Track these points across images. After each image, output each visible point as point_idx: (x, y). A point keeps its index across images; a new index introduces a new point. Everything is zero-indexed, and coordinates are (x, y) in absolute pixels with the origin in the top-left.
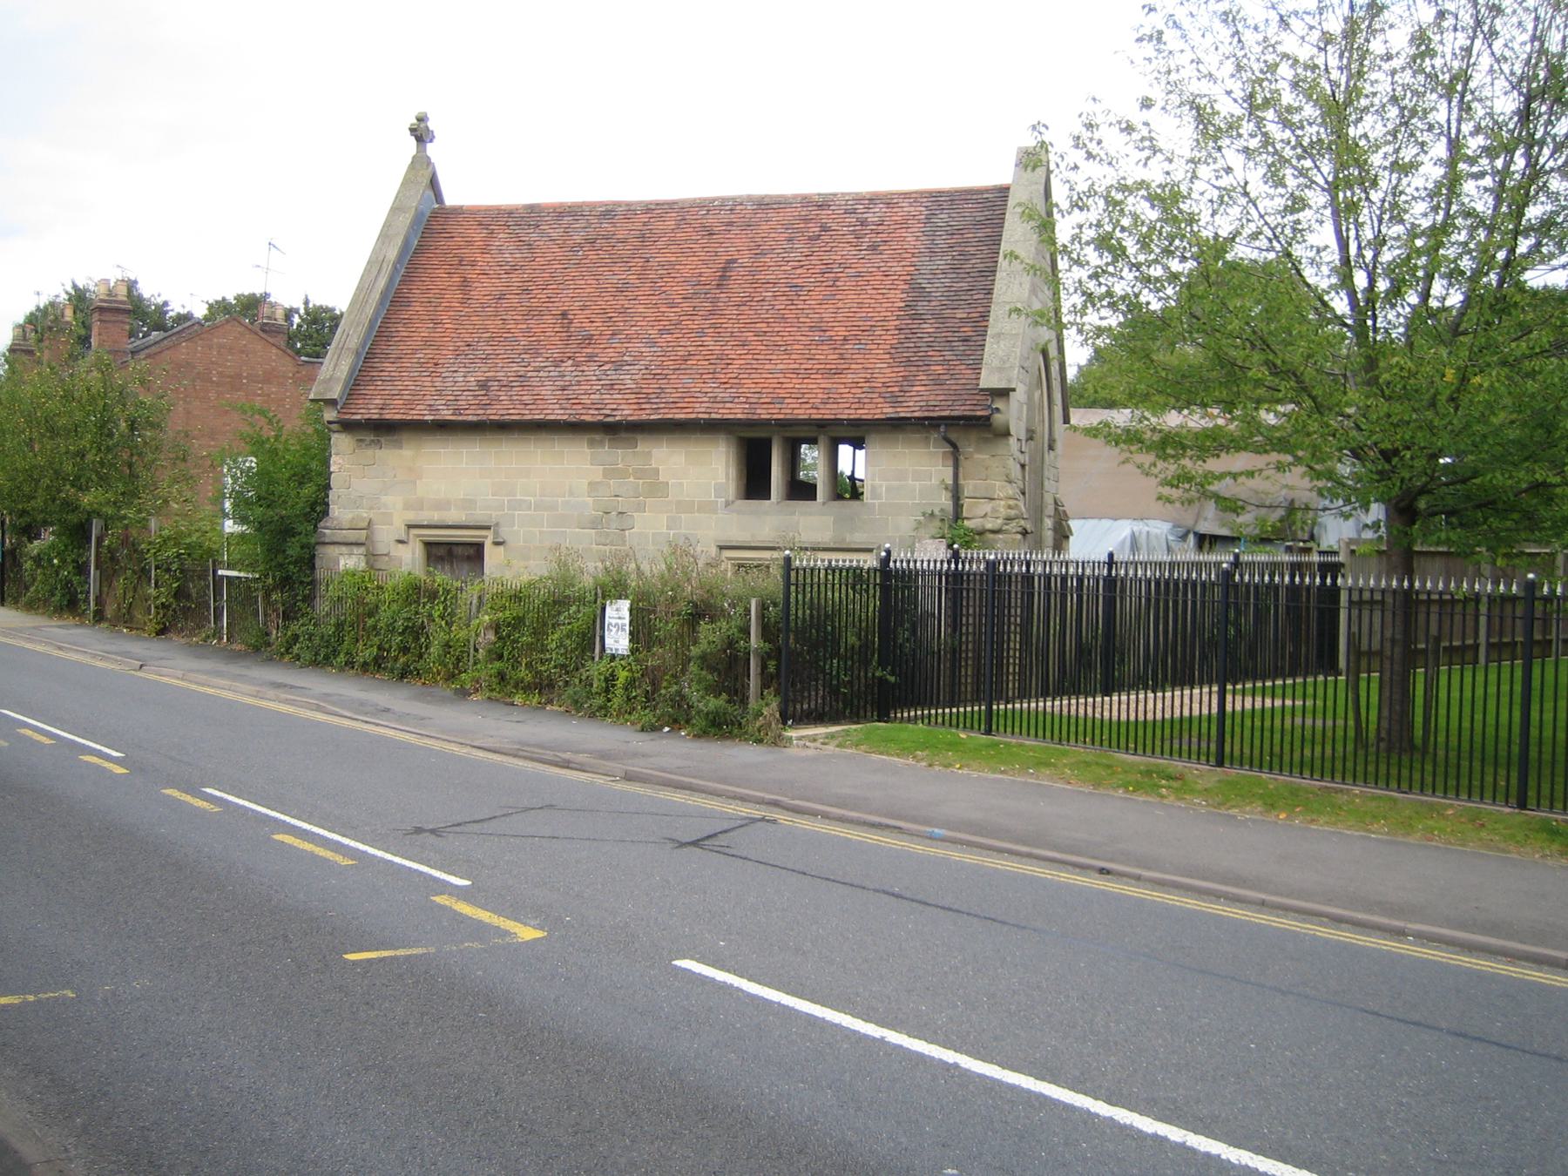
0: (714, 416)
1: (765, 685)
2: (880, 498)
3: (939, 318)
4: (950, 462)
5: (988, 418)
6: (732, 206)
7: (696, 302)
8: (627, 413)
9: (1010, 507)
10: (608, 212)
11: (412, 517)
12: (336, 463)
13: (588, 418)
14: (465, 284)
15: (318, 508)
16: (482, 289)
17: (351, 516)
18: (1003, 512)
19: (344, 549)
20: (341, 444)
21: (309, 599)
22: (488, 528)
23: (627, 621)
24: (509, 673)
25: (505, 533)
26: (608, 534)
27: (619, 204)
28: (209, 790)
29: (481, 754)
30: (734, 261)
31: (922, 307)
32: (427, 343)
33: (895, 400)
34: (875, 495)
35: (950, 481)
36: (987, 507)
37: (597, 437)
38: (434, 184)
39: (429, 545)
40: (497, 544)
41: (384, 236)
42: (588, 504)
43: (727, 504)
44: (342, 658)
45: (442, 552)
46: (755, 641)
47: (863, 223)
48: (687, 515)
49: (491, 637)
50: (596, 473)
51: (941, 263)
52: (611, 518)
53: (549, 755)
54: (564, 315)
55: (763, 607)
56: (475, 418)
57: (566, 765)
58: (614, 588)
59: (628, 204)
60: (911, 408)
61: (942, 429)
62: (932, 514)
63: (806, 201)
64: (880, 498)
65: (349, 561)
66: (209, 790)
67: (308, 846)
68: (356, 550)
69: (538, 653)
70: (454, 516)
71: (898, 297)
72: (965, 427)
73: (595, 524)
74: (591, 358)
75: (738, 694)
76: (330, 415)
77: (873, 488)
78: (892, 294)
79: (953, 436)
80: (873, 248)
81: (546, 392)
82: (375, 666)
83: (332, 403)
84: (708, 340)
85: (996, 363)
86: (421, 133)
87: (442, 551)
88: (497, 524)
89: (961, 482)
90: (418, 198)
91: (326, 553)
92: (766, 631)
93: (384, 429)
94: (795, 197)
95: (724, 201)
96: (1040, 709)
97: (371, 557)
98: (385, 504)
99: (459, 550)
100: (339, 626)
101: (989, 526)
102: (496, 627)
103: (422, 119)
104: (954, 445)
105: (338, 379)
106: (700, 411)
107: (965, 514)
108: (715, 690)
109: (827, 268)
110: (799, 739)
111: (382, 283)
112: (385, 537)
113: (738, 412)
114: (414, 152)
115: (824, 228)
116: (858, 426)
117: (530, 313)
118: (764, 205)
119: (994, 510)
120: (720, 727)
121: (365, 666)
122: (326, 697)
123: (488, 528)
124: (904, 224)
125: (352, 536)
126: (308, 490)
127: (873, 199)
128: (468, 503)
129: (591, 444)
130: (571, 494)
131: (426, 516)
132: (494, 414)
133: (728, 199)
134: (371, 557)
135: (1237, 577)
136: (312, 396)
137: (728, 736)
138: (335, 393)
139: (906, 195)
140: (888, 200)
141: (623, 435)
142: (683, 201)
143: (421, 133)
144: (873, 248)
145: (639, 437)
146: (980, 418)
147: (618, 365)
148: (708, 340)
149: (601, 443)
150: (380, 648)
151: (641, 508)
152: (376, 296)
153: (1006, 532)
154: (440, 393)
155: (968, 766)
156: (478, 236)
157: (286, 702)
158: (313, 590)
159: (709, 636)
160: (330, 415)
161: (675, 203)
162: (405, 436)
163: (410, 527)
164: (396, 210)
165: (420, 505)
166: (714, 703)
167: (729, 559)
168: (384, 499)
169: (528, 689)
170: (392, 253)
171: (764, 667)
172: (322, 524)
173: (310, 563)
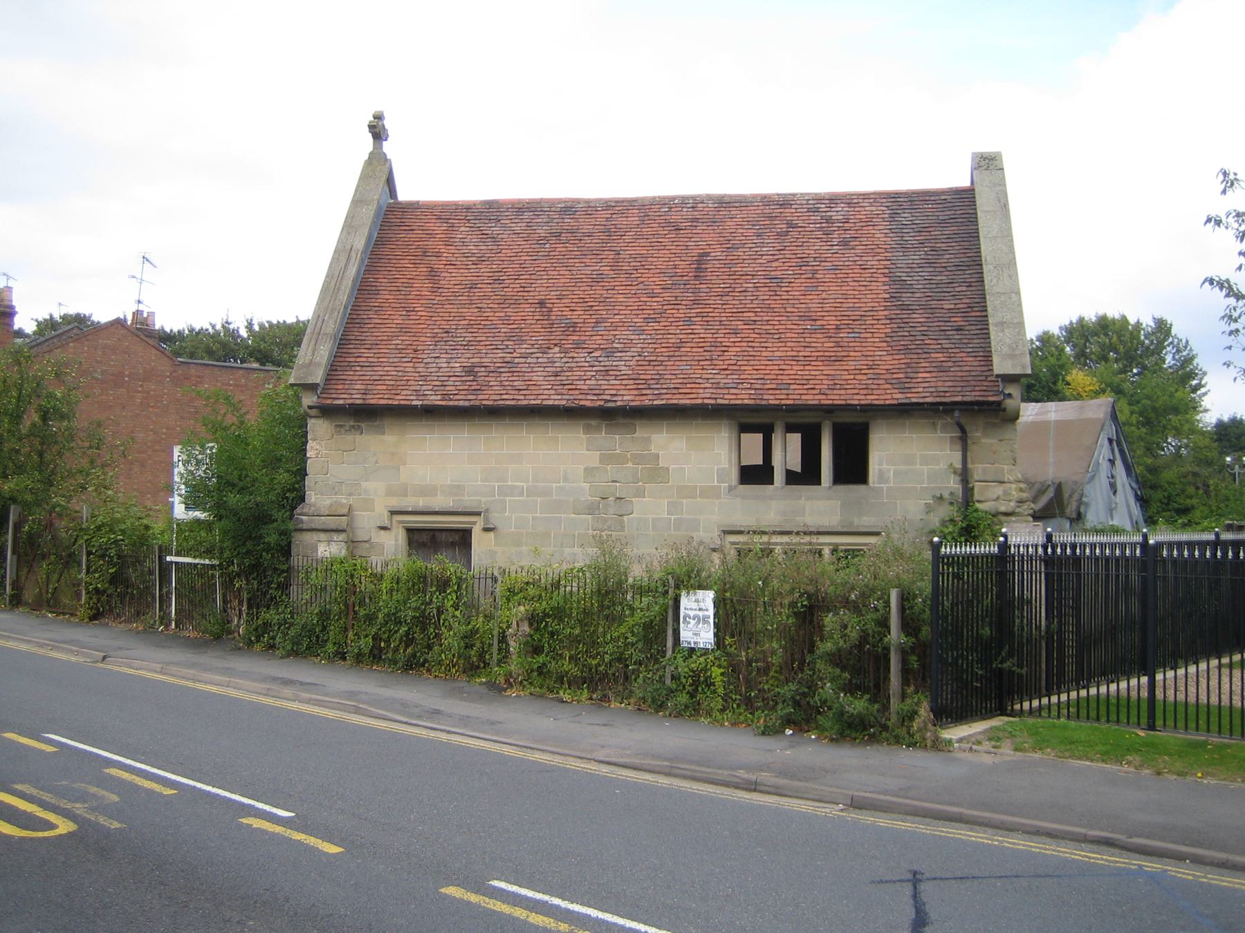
0: (720, 401)
1: (905, 681)
2: (887, 481)
3: (925, 308)
4: (959, 447)
5: (999, 403)
6: (694, 203)
7: (677, 293)
8: (627, 398)
9: (1021, 490)
10: (569, 208)
11: (396, 503)
12: (312, 448)
13: (588, 404)
14: (433, 274)
15: (295, 495)
16: (450, 279)
17: (328, 502)
18: (1015, 495)
19: (323, 536)
20: (319, 429)
21: (285, 587)
22: (479, 514)
23: (711, 612)
24: (552, 666)
25: (496, 519)
26: (605, 520)
27: (578, 201)
28: (496, 883)
29: (605, 769)
30: (707, 254)
31: (906, 298)
32: (403, 330)
33: (903, 387)
34: (882, 477)
35: (958, 465)
36: (999, 490)
37: (593, 423)
38: (390, 182)
39: (410, 531)
40: (487, 530)
41: (349, 226)
42: (584, 490)
43: (731, 489)
44: (330, 648)
45: (423, 539)
46: (895, 635)
47: (829, 220)
48: (684, 502)
49: (525, 628)
50: (593, 458)
51: (915, 258)
52: (608, 505)
53: (724, 774)
54: (542, 303)
55: (905, 598)
56: (466, 404)
57: (753, 787)
58: (688, 579)
59: (587, 201)
60: (922, 393)
61: (957, 414)
62: (941, 498)
63: (766, 200)
64: (887, 481)
65: (328, 549)
66: (496, 883)
67: (505, 908)
68: (335, 537)
69: (592, 644)
70: (439, 502)
71: (881, 288)
72: (975, 413)
73: (591, 509)
74: (578, 346)
75: (878, 691)
76: (308, 400)
77: (881, 473)
78: (874, 286)
79: (963, 421)
80: (844, 243)
81: (538, 377)
82: (374, 657)
83: (312, 387)
84: (698, 329)
85: (1005, 350)
86: (378, 131)
87: (424, 537)
88: (487, 510)
89: (970, 466)
90: (377, 193)
91: (303, 541)
92: (909, 625)
93: (366, 415)
94: (755, 196)
95: (684, 200)
96: (1123, 693)
97: (352, 543)
98: (365, 492)
99: (444, 536)
100: (324, 615)
101: (1003, 509)
102: (533, 619)
103: (379, 117)
104: (963, 431)
105: (319, 364)
106: (705, 396)
107: (977, 496)
108: (850, 689)
109: (803, 262)
110: (960, 740)
111: (352, 271)
112: (366, 523)
113: (744, 398)
114: (371, 149)
115: (791, 225)
116: (865, 411)
117: (504, 302)
118: (724, 203)
119: (1006, 493)
120: (854, 730)
121: (359, 658)
122: (351, 695)
123: (479, 514)
124: (869, 221)
125: (332, 522)
126: (283, 477)
127: (833, 200)
128: (457, 489)
129: (588, 429)
130: (566, 479)
131: (410, 502)
132: (488, 398)
133: (688, 198)
134: (352, 543)
135: (1165, 553)
136: (292, 381)
137: (873, 739)
138: (318, 377)
139: (865, 196)
140: (851, 200)
141: (621, 421)
142: (643, 199)
143: (378, 131)
144: (844, 243)
145: (638, 422)
146: (993, 402)
147: (610, 353)
148: (698, 329)
149: (598, 429)
150: (376, 638)
151: (640, 493)
152: (348, 284)
153: (1018, 514)
154: (424, 378)
155: (1213, 775)
156: (439, 229)
157: (309, 701)
158: (288, 579)
159: (838, 628)
160: (308, 400)
161: (635, 200)
162: (387, 422)
163: (393, 513)
164: (357, 202)
165: (404, 491)
166: (858, 705)
167: (733, 543)
168: (364, 484)
169: (575, 683)
170: (360, 243)
171: (904, 662)
172: (298, 510)
173: (286, 551)
